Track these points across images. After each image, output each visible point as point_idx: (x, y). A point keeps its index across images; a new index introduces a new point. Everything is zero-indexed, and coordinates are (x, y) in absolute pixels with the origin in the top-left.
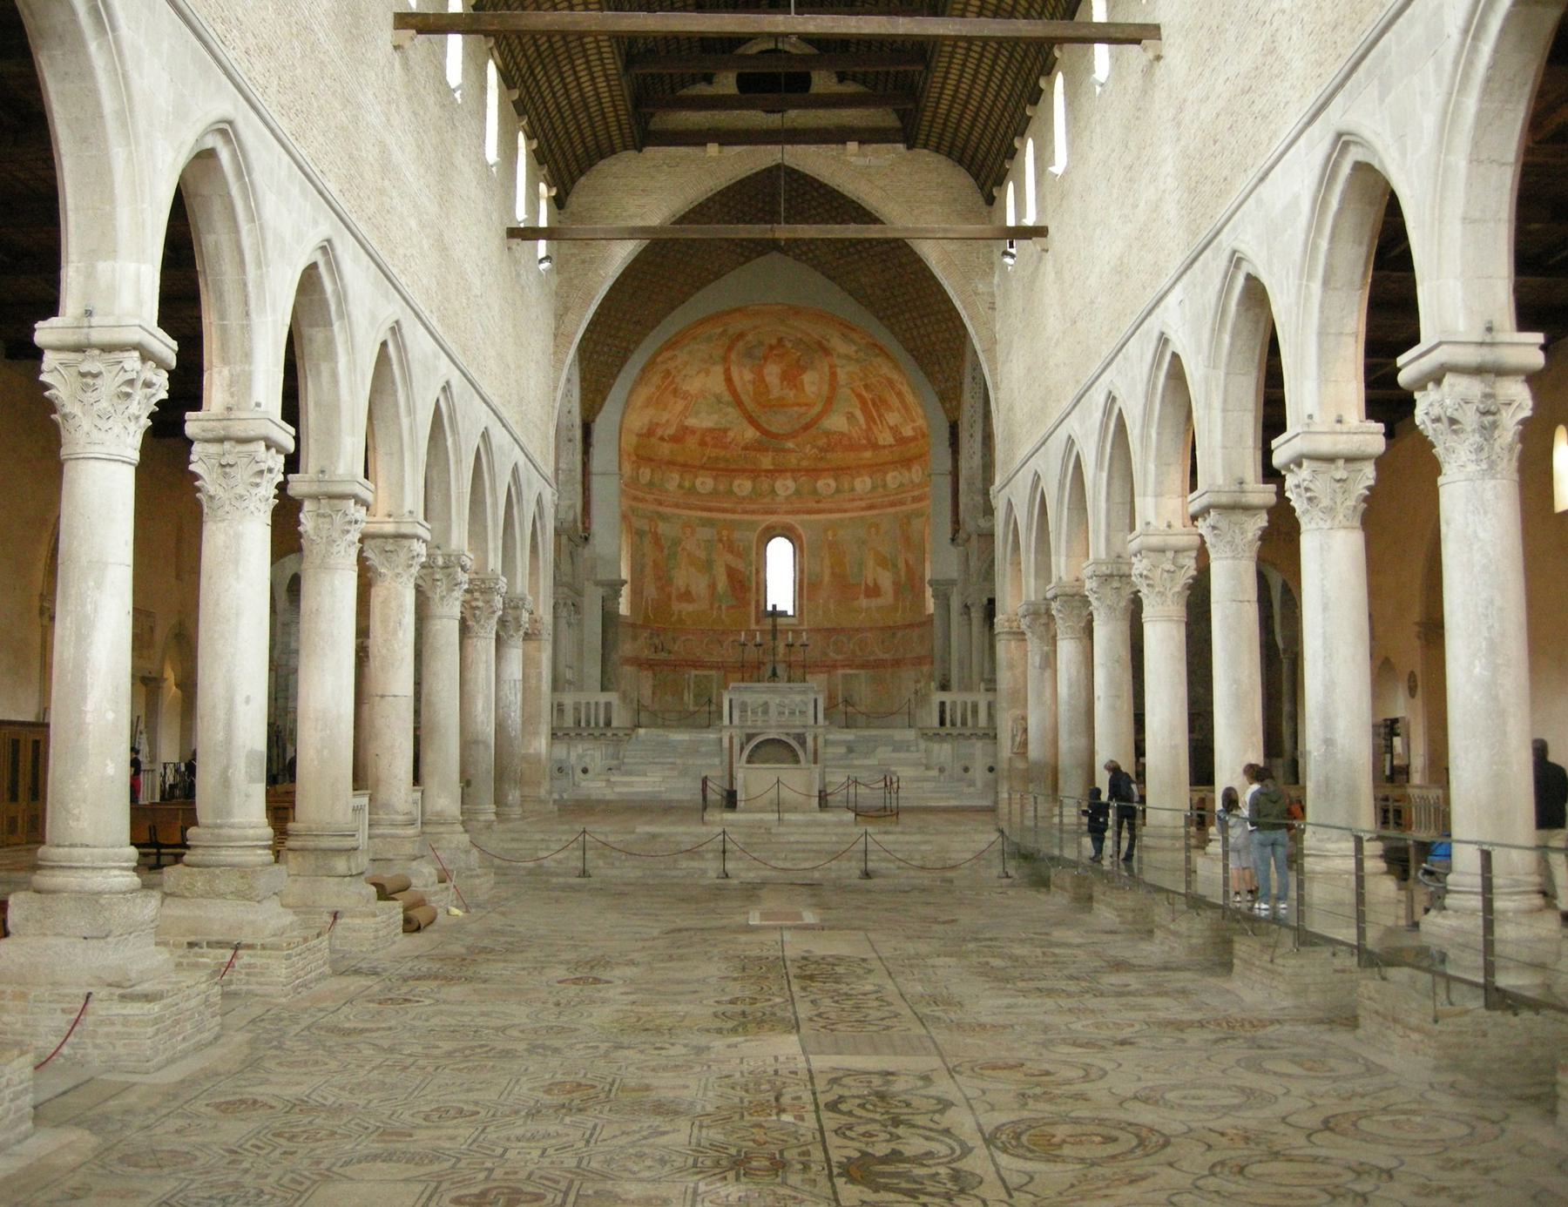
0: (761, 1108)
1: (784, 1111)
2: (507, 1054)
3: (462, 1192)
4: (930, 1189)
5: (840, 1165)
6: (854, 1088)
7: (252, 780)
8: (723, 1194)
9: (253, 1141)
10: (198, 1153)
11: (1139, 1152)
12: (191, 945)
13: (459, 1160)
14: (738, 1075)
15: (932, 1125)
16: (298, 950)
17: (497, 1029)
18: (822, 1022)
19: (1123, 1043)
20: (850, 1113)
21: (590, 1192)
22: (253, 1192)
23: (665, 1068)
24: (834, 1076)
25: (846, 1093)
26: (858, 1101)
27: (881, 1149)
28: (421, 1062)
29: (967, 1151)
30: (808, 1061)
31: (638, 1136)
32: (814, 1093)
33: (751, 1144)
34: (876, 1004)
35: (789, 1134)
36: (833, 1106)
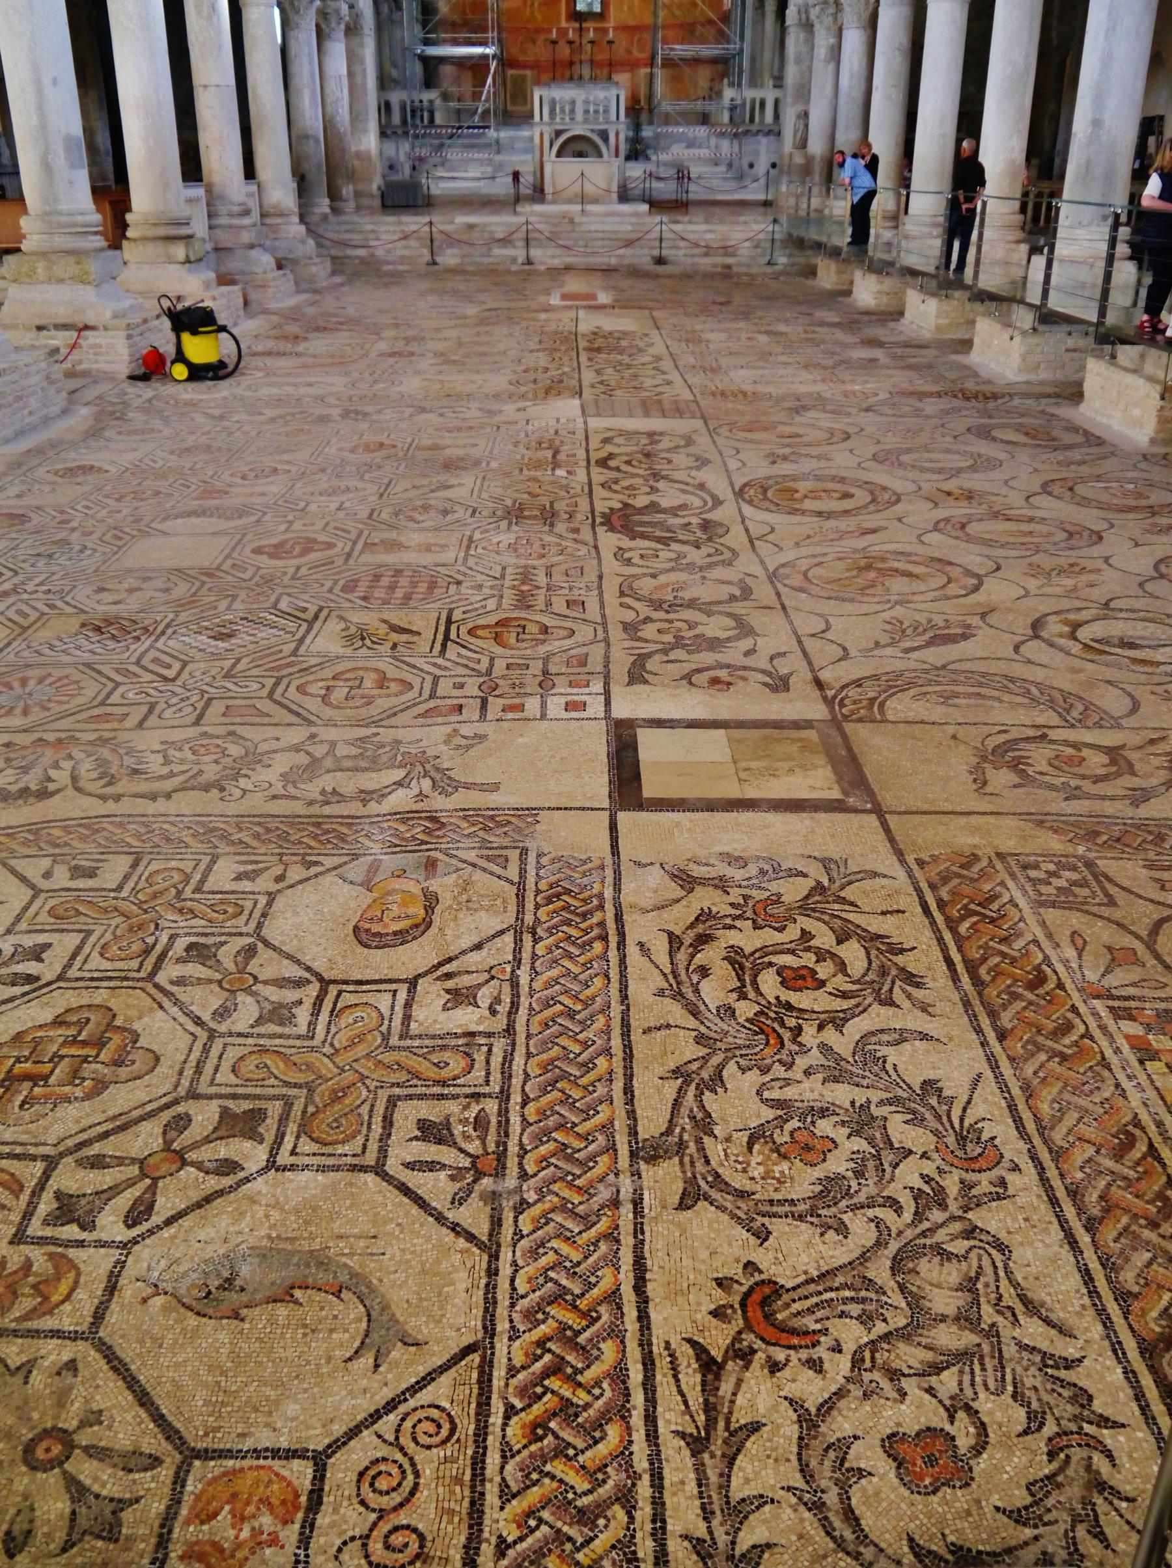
0: (538, 465)
1: (559, 466)
2: (323, 419)
3: (262, 543)
4: (681, 537)
5: (603, 515)
6: (621, 448)
7: (73, 166)
8: (495, 540)
9: (85, 503)
10: (31, 514)
11: (872, 508)
12: (40, 328)
13: (265, 514)
14: (523, 435)
15: (689, 480)
16: (138, 330)
17: (316, 398)
18: (602, 388)
19: (867, 410)
20: (618, 469)
21: (376, 541)
22: (78, 548)
23: (459, 429)
24: (607, 435)
25: (616, 450)
26: (626, 458)
27: (641, 501)
28: (245, 428)
29: (718, 502)
30: (585, 422)
31: (426, 490)
32: (587, 451)
33: (526, 496)
34: (652, 372)
35: (562, 487)
36: (603, 463)
